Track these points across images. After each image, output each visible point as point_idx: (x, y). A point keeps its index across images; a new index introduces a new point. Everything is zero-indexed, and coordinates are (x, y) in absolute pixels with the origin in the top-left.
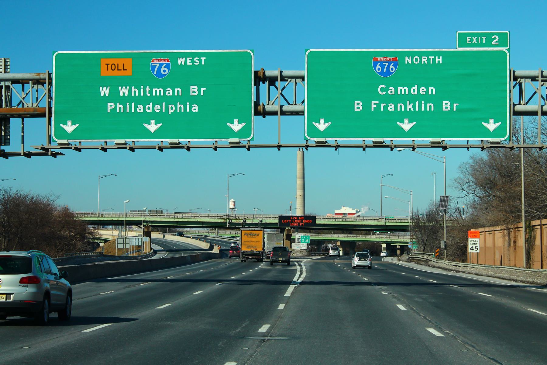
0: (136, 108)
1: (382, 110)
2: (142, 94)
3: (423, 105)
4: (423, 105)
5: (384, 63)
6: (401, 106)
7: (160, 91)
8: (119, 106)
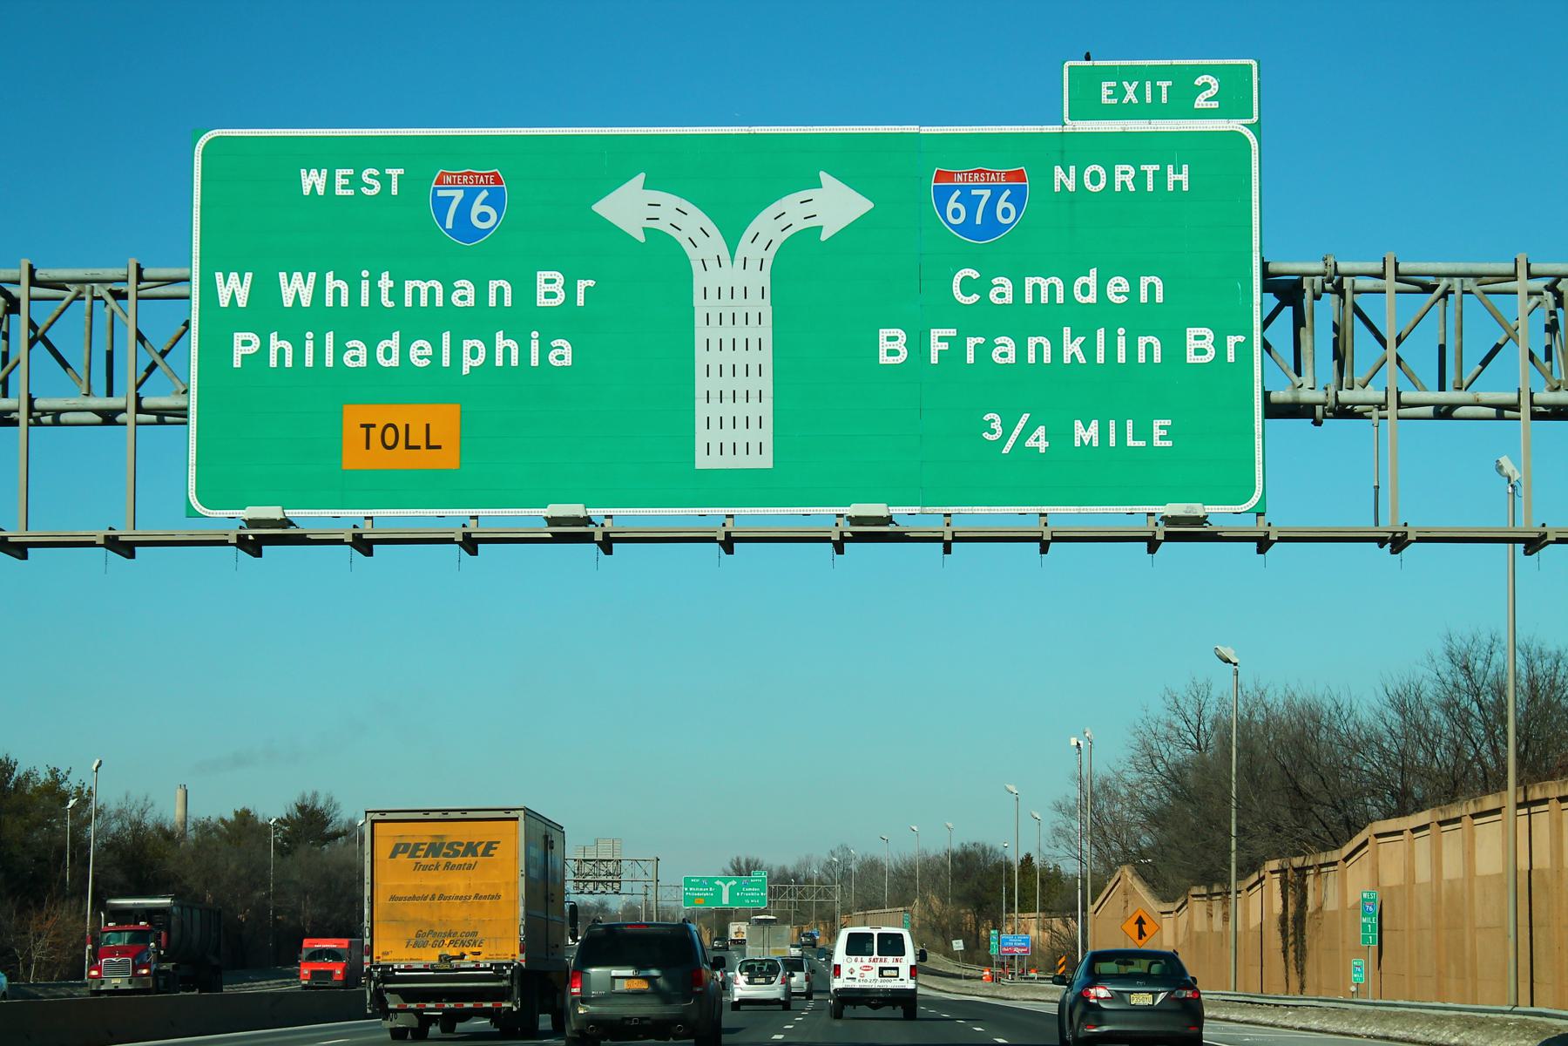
0: (340, 350)
1: (970, 359)
2: (365, 302)
3: (1121, 341)
4: (1121, 341)
5: (974, 192)
6: (1039, 347)
7: (432, 291)
8: (275, 343)
